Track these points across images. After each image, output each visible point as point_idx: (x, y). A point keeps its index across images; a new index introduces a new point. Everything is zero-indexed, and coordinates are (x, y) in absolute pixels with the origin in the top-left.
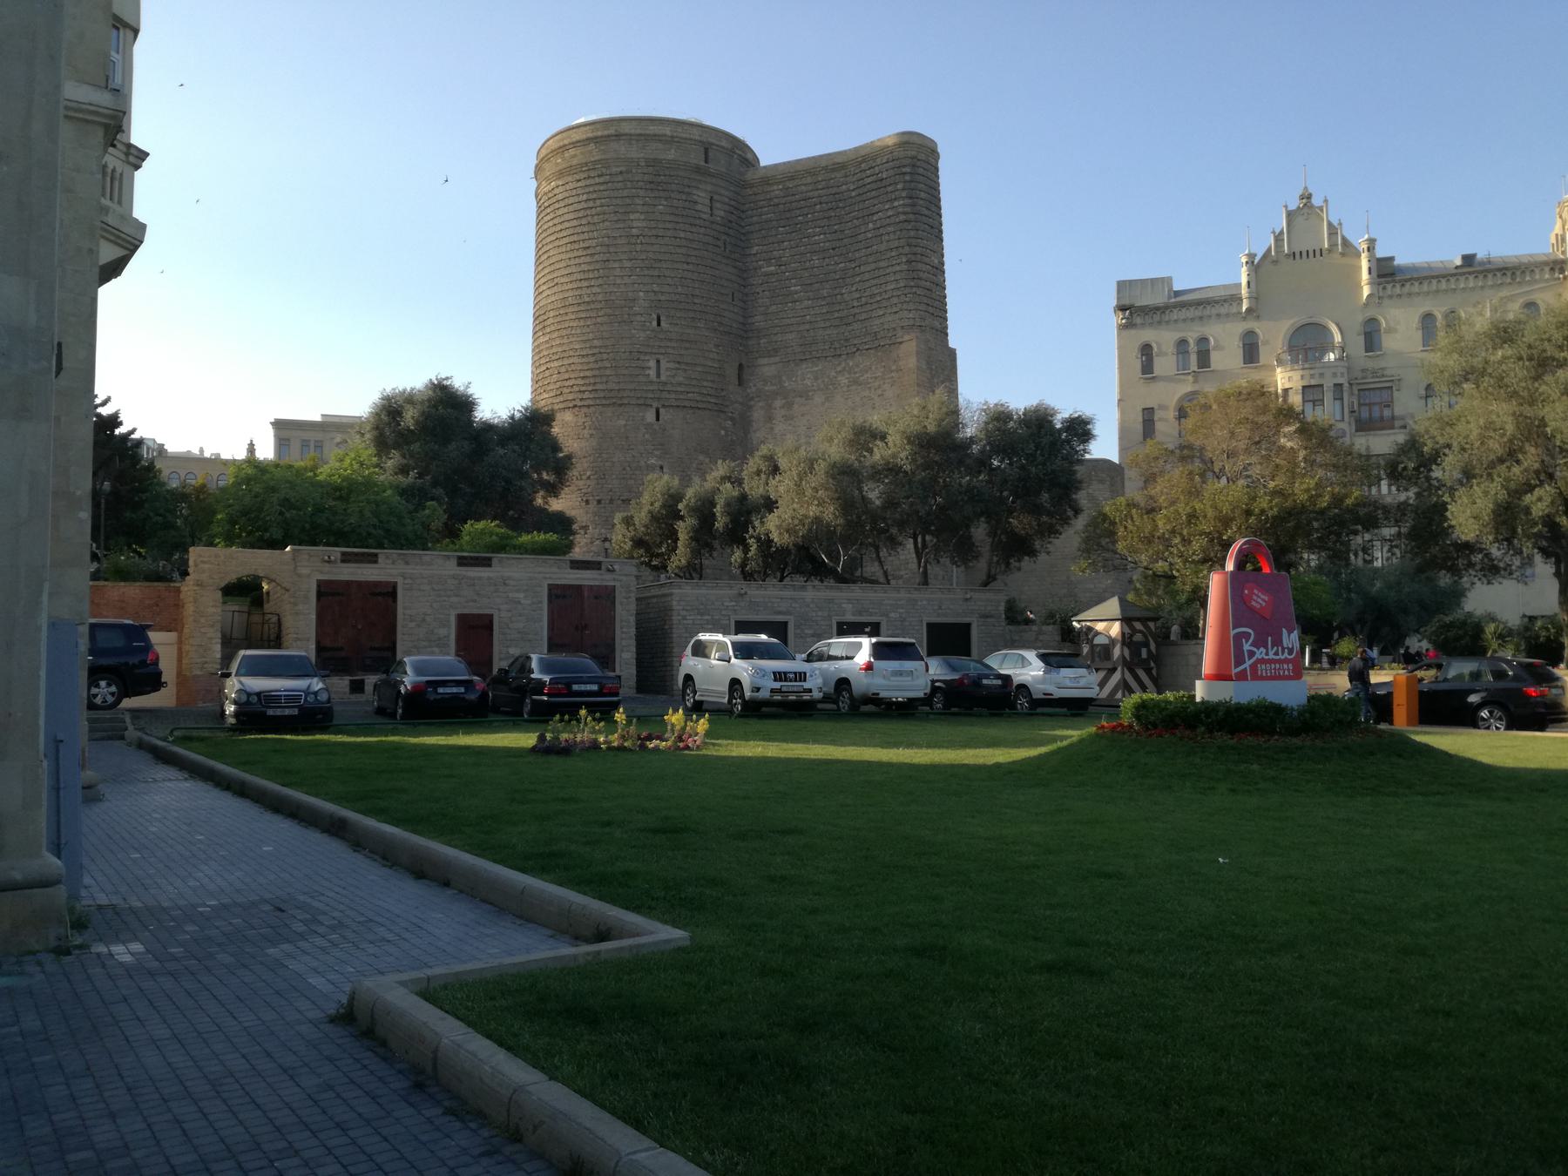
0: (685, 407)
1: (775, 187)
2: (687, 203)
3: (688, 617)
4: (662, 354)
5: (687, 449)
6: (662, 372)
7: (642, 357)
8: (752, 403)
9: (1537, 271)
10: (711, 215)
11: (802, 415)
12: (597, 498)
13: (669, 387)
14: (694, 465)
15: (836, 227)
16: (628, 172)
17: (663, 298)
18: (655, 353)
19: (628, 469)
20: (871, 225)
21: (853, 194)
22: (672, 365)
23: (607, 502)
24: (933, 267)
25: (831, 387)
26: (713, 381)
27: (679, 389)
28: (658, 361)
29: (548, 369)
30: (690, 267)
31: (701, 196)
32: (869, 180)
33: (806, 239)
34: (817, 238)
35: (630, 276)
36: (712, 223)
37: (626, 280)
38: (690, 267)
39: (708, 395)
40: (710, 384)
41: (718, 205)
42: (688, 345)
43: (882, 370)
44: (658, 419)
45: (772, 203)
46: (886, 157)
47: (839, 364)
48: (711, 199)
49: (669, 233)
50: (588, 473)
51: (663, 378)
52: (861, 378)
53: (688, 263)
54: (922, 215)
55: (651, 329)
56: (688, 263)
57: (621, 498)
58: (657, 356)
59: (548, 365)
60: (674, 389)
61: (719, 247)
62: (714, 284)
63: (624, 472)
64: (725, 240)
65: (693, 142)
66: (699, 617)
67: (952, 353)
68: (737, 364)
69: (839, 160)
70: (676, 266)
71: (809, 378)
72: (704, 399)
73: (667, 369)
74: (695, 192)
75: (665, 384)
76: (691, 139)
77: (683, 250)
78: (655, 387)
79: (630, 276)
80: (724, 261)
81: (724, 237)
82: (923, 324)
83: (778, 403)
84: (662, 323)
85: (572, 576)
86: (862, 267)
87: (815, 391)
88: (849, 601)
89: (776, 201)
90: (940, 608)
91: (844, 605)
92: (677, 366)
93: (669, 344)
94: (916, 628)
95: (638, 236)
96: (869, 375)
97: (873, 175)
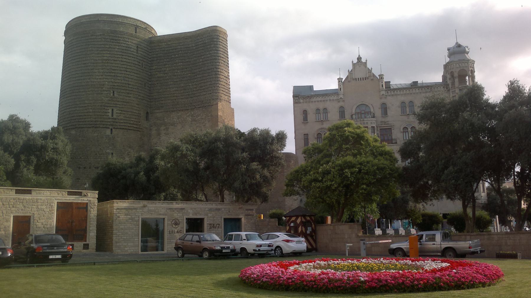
0: (123, 129)
1: (163, 44)
3: (120, 217)
4: (114, 107)
5: (124, 146)
6: (114, 114)
7: (106, 108)
8: (152, 128)
9: (439, 87)
11: (173, 133)
12: (84, 166)
13: (117, 121)
14: (126, 153)
15: (187, 60)
16: (103, 35)
17: (116, 84)
18: (111, 107)
19: (98, 154)
20: (201, 60)
21: (194, 48)
22: (118, 112)
23: (88, 168)
24: (225, 77)
25: (184, 122)
26: (136, 119)
27: (121, 121)
28: (113, 110)
29: (65, 112)
30: (128, 73)
32: (201, 43)
33: (175, 64)
34: (179, 64)
35: (102, 75)
36: (137, 56)
37: (100, 77)
38: (128, 73)
40: (134, 120)
41: (140, 49)
42: (125, 104)
43: (205, 115)
44: (111, 133)
45: (162, 50)
46: (207, 35)
47: (188, 113)
48: (137, 47)
49: (120, 59)
50: (81, 156)
51: (115, 117)
52: (197, 119)
53: (127, 71)
54: (221, 57)
55: (110, 97)
56: (127, 71)
57: (94, 166)
58: (112, 108)
59: (66, 111)
60: (119, 121)
61: (140, 66)
63: (96, 155)
64: (142, 63)
66: (125, 217)
67: (233, 109)
68: (146, 112)
69: (188, 35)
71: (175, 118)
72: (132, 126)
76: (129, 24)
79: (102, 75)
81: (141, 62)
83: (163, 128)
84: (115, 95)
85: (68, 198)
86: (197, 76)
87: (178, 123)
88: (191, 209)
89: (163, 49)
90: (229, 212)
91: (189, 211)
92: (120, 112)
94: (220, 220)
95: (106, 60)
96: (199, 118)
97: (202, 41)
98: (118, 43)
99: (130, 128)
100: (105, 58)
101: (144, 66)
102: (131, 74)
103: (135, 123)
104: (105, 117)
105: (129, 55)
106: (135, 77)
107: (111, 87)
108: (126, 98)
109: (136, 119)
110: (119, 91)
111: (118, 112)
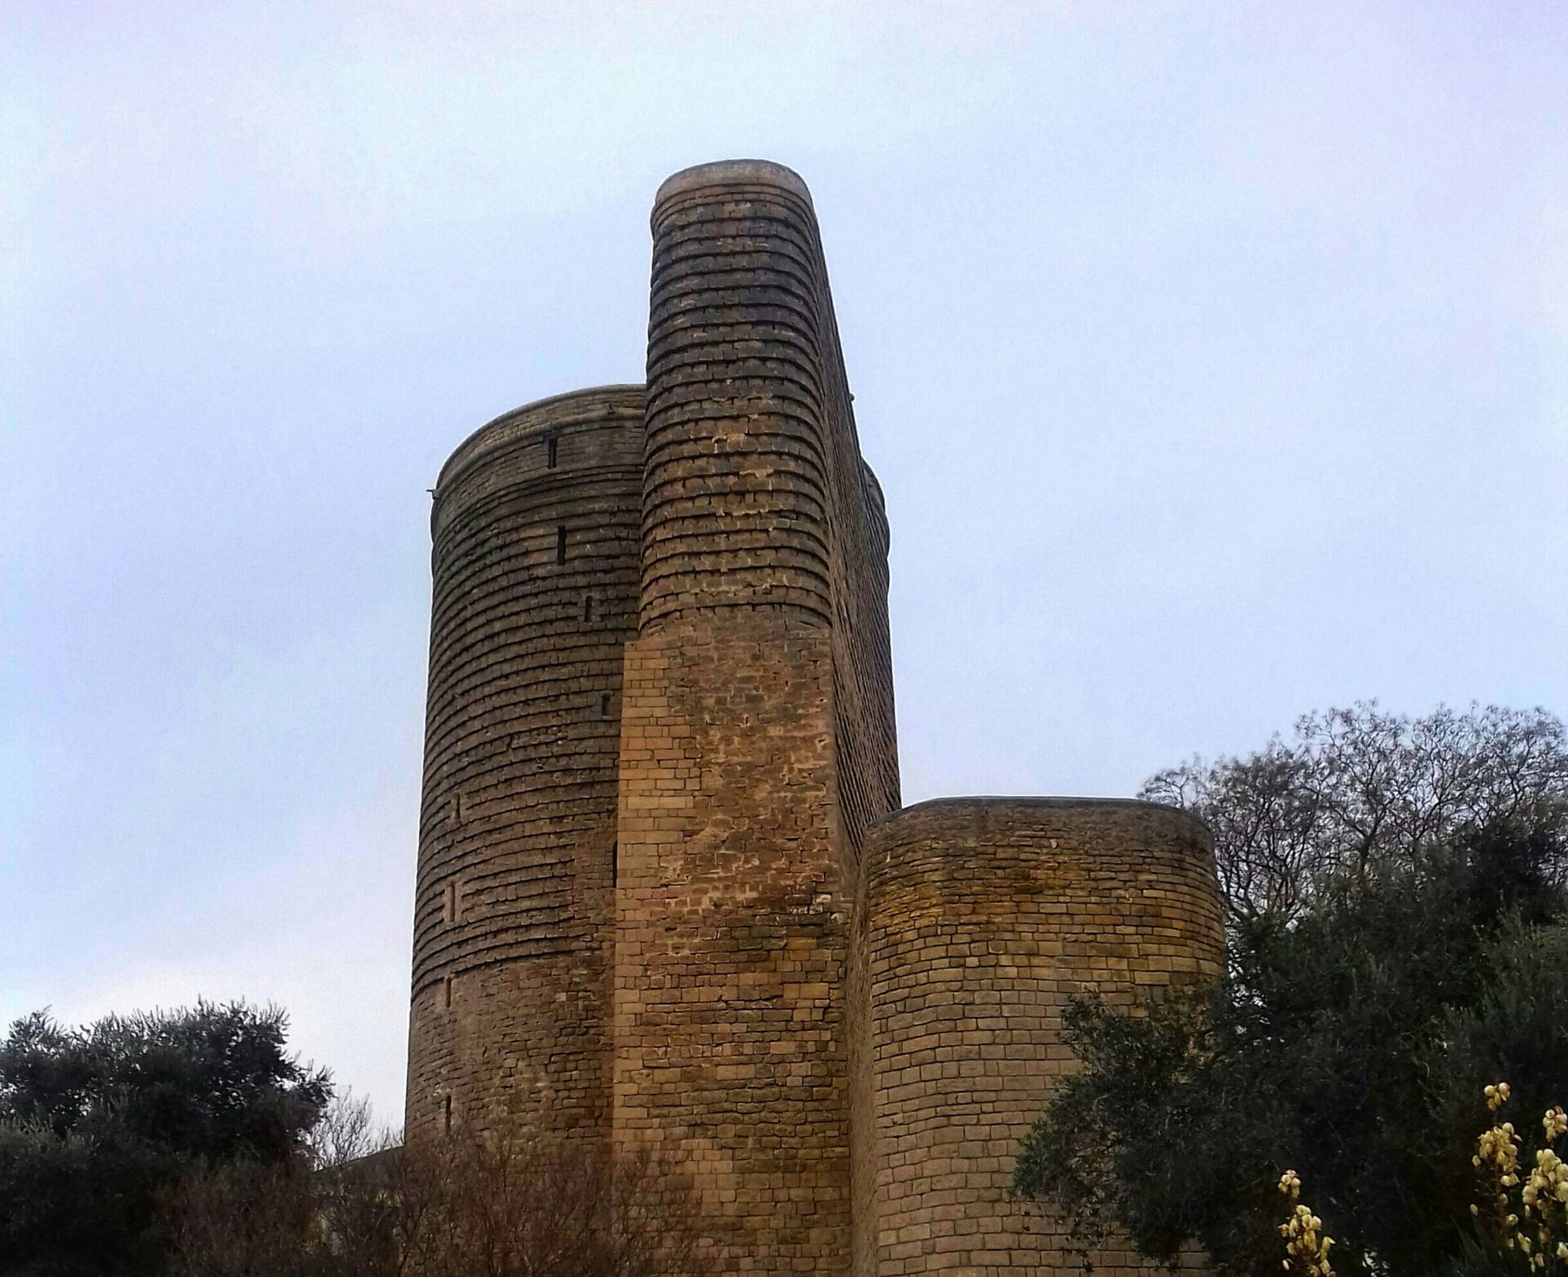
0: (487, 965)
2: (513, 560)
10: (562, 560)
13: (469, 933)
14: (497, 1081)
31: (541, 537)
36: (562, 575)
39: (531, 925)
40: (535, 903)
44: (448, 1005)
48: (563, 533)
49: (480, 634)
51: (458, 917)
53: (507, 676)
56: (507, 676)
61: (574, 618)
62: (557, 697)
70: (487, 690)
74: (522, 536)
80: (582, 641)
82: (671, 605)
93: (469, 847)
99: (513, 953)
101: (598, 611)
103: (540, 917)
104: (438, 930)
106: (547, 686)
108: (496, 808)
109: (541, 895)
111: (469, 889)
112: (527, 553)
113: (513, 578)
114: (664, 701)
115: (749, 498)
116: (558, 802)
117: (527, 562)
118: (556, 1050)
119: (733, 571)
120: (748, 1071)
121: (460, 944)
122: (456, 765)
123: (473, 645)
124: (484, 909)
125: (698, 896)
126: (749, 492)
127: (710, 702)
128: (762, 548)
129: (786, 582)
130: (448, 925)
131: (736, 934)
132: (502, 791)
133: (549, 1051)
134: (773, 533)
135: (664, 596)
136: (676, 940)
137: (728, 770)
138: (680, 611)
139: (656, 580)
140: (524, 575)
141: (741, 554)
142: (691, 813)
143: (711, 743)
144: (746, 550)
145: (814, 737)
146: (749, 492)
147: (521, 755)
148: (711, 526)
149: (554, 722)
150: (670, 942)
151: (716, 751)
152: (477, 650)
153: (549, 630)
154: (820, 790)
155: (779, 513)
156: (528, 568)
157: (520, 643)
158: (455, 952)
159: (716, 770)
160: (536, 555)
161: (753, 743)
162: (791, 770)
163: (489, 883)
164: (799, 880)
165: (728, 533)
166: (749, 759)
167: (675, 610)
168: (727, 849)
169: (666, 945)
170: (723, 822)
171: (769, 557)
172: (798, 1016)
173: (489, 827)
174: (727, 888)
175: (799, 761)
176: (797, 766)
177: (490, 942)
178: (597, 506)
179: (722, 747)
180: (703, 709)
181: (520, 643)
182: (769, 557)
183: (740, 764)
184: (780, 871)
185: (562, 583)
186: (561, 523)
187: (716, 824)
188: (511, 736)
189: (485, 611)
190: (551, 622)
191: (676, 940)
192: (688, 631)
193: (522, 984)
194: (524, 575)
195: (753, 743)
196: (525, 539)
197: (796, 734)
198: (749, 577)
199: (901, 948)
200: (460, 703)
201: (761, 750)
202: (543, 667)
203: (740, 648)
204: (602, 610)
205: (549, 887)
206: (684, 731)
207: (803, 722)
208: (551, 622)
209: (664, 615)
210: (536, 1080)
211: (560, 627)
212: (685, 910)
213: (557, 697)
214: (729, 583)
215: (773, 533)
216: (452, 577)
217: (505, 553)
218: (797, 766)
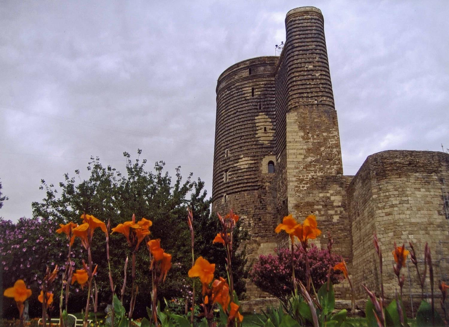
7: (222, 173)
16: (223, 94)
17: (229, 143)
26: (250, 175)
27: (233, 184)
38: (241, 124)
40: (249, 177)
44: (225, 202)
48: (253, 89)
49: (232, 113)
51: (228, 180)
56: (240, 122)
61: (257, 109)
64: (260, 104)
65: (243, 69)
73: (229, 175)
74: (243, 90)
75: (228, 183)
77: (237, 118)
78: (225, 186)
82: (297, 105)
84: (229, 155)
92: (233, 173)
98: (232, 95)
99: (243, 189)
100: (222, 119)
102: (246, 123)
104: (222, 184)
105: (242, 103)
106: (250, 125)
107: (225, 147)
109: (250, 175)
110: (232, 148)
112: (244, 94)
113: (240, 100)
114: (297, 127)
115: (315, 80)
116: (254, 152)
117: (244, 96)
118: (256, 213)
119: (312, 97)
120: (323, 218)
121: (228, 187)
122: (226, 143)
123: (230, 115)
124: (235, 178)
125: (308, 174)
126: (314, 79)
127: (308, 127)
128: (319, 92)
129: (325, 99)
130: (225, 182)
131: (318, 184)
132: (239, 149)
133: (253, 214)
134: (321, 88)
135: (295, 103)
136: (303, 185)
137: (313, 143)
138: (299, 106)
139: (293, 99)
140: (243, 99)
141: (314, 93)
142: (305, 154)
143: (309, 137)
144: (315, 92)
145: (334, 136)
146: (314, 79)
147: (244, 141)
148: (306, 86)
149: (252, 133)
150: (301, 186)
151: (310, 139)
152: (232, 116)
153: (250, 111)
154: (337, 148)
155: (322, 84)
156: (244, 97)
157: (243, 114)
158: (227, 189)
159: (311, 144)
160: (246, 94)
161: (320, 137)
162: (329, 144)
163: (236, 172)
164: (333, 171)
165: (310, 88)
166: (319, 141)
167: (298, 106)
168: (315, 163)
169: (300, 186)
170: (313, 156)
171: (321, 94)
172: (335, 204)
173: (236, 158)
174: (315, 172)
175: (331, 141)
176: (331, 143)
177: (236, 186)
178: (261, 83)
179: (311, 138)
180: (307, 129)
181: (243, 114)
182: (321, 94)
183: (317, 142)
184: (328, 168)
185: (253, 101)
186: (253, 87)
187: (311, 157)
188: (241, 136)
189: (233, 107)
190: (251, 110)
191: (303, 185)
192: (301, 110)
193: (245, 197)
194: (243, 99)
195: (320, 137)
196: (244, 91)
197: (330, 135)
198: (316, 98)
199: (381, 186)
200: (227, 129)
201: (321, 139)
202: (249, 120)
203: (314, 115)
204: (264, 107)
205: (252, 173)
206: (302, 134)
207: (332, 132)
208: (251, 110)
209: (295, 107)
210: (250, 221)
211: (253, 111)
212: (305, 178)
213: (253, 127)
214: (311, 99)
215: (321, 88)
216: (224, 100)
217: (238, 94)
218: (331, 143)
